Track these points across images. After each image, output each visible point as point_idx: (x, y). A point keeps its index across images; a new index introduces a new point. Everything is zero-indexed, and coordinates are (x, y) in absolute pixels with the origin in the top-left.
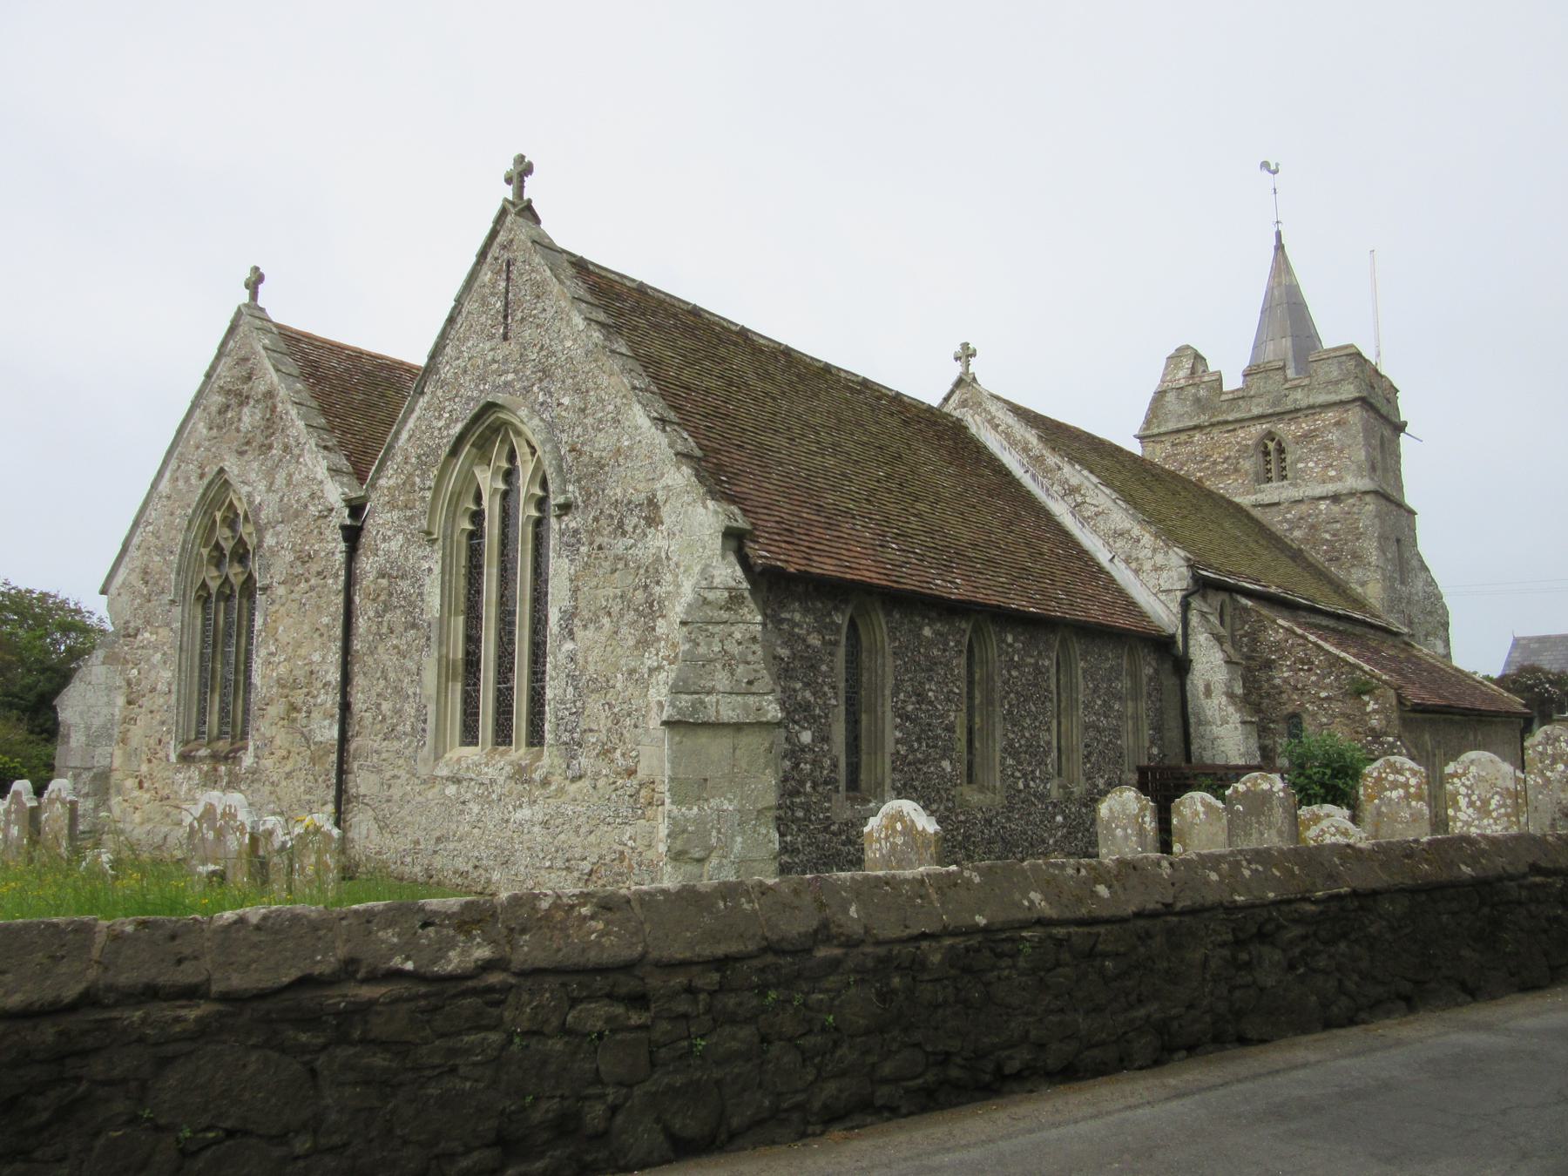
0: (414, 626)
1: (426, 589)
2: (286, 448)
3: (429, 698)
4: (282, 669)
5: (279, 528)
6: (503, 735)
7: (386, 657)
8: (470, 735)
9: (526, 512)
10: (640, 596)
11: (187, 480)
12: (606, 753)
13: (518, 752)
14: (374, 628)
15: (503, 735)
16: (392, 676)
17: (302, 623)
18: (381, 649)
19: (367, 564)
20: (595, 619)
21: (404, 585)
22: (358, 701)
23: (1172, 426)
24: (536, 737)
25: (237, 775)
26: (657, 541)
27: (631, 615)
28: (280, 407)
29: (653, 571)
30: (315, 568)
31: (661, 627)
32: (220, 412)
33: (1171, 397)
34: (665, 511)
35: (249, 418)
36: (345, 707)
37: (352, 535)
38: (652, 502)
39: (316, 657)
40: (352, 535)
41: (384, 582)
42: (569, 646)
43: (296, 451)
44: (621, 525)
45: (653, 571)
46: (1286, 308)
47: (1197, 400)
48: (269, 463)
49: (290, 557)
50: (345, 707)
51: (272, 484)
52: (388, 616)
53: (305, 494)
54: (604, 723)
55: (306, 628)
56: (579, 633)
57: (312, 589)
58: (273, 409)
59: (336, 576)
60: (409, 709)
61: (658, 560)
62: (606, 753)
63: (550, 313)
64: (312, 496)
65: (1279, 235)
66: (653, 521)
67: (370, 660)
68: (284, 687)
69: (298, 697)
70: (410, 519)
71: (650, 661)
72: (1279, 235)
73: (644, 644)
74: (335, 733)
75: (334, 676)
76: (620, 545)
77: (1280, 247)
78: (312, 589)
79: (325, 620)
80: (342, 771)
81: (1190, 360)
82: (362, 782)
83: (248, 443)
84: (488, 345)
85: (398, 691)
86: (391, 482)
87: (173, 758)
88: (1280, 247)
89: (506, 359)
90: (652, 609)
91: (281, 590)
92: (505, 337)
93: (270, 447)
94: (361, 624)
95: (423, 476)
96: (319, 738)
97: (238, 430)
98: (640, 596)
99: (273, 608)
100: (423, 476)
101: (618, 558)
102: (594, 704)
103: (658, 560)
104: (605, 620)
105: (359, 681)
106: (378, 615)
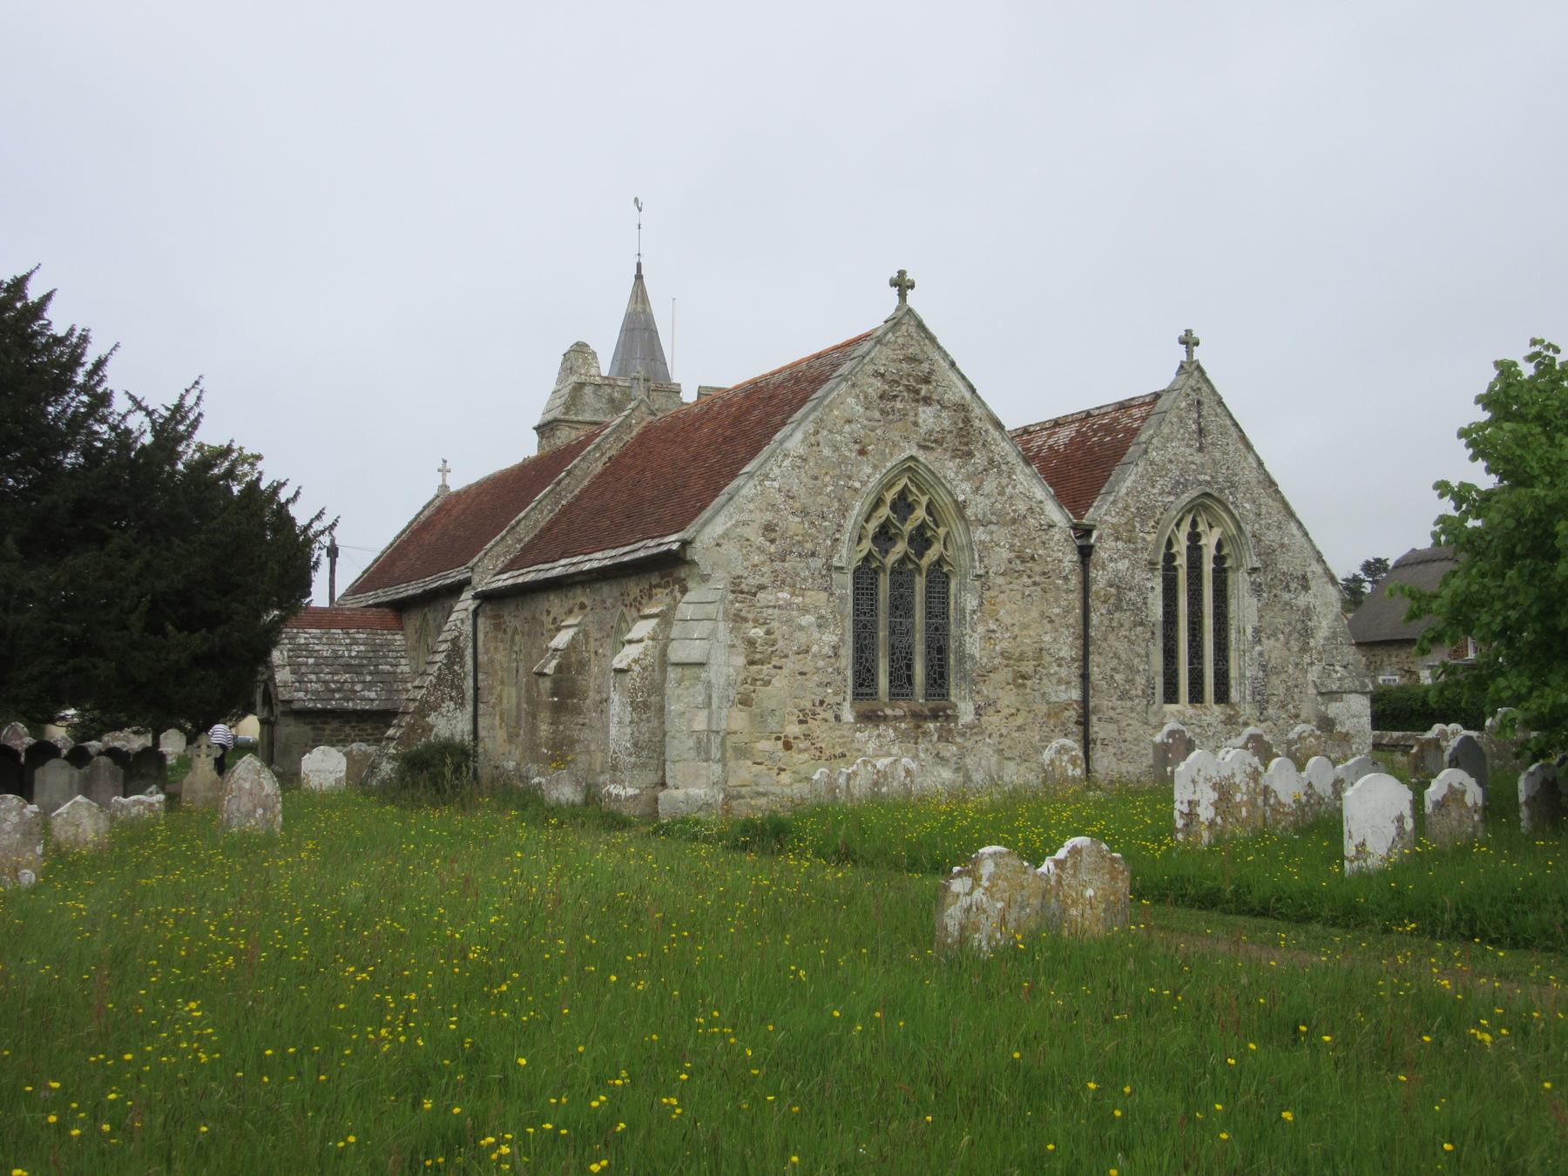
0: (1141, 624)
1: (1150, 601)
2: (991, 461)
3: (1156, 673)
4: (1005, 644)
5: (993, 527)
6: (1196, 696)
7: (1116, 644)
8: (1171, 695)
9: (1208, 567)
10: (1299, 626)
11: (836, 449)
12: (1283, 706)
13: (1183, 705)
14: (1106, 623)
15: (1196, 696)
16: (1123, 656)
17: (1028, 610)
18: (1111, 637)
19: (1100, 578)
20: (1274, 635)
21: (1132, 595)
22: (1095, 672)
23: (588, 417)
24: (1222, 696)
25: (950, 731)
26: (1303, 600)
27: (1296, 635)
28: (977, 423)
29: (1308, 612)
30: (1037, 569)
31: (1312, 643)
32: (881, 397)
33: (588, 390)
34: (1312, 584)
35: (926, 416)
36: (1085, 677)
37: (1085, 553)
38: (1304, 577)
39: (1047, 638)
40: (1085, 553)
41: (1113, 590)
42: (1258, 648)
43: (1004, 467)
44: (1287, 586)
45: (1308, 612)
46: (639, 331)
47: (611, 400)
48: (971, 469)
49: (1006, 554)
50: (1085, 677)
51: (978, 489)
52: (1117, 615)
53: (1022, 507)
54: (1281, 690)
55: (1035, 614)
56: (1264, 640)
57: (1035, 584)
58: (967, 421)
59: (1066, 579)
60: (1140, 681)
61: (1308, 608)
62: (1283, 706)
63: (1232, 448)
64: (1031, 509)
65: (639, 266)
66: (1306, 588)
67: (1104, 645)
68: (1009, 659)
69: (1027, 667)
70: (1135, 551)
71: (1307, 659)
72: (639, 266)
73: (1305, 649)
74: (1075, 694)
75: (1067, 648)
76: (1286, 596)
77: (639, 277)
78: (1035, 584)
79: (1057, 611)
80: (1084, 722)
81: (580, 353)
82: (1098, 729)
83: (935, 441)
84: (1188, 451)
85: (1130, 668)
86: (1114, 520)
87: (848, 715)
88: (639, 277)
89: (1203, 465)
90: (1307, 633)
91: (1000, 580)
92: (1201, 449)
93: (970, 454)
94: (1095, 619)
95: (1143, 523)
96: (1053, 699)
97: (916, 424)
98: (1299, 626)
99: (987, 594)
100: (1143, 523)
101: (1286, 604)
102: (1275, 680)
103: (1308, 608)
104: (1281, 636)
105: (1094, 658)
106: (1109, 612)
